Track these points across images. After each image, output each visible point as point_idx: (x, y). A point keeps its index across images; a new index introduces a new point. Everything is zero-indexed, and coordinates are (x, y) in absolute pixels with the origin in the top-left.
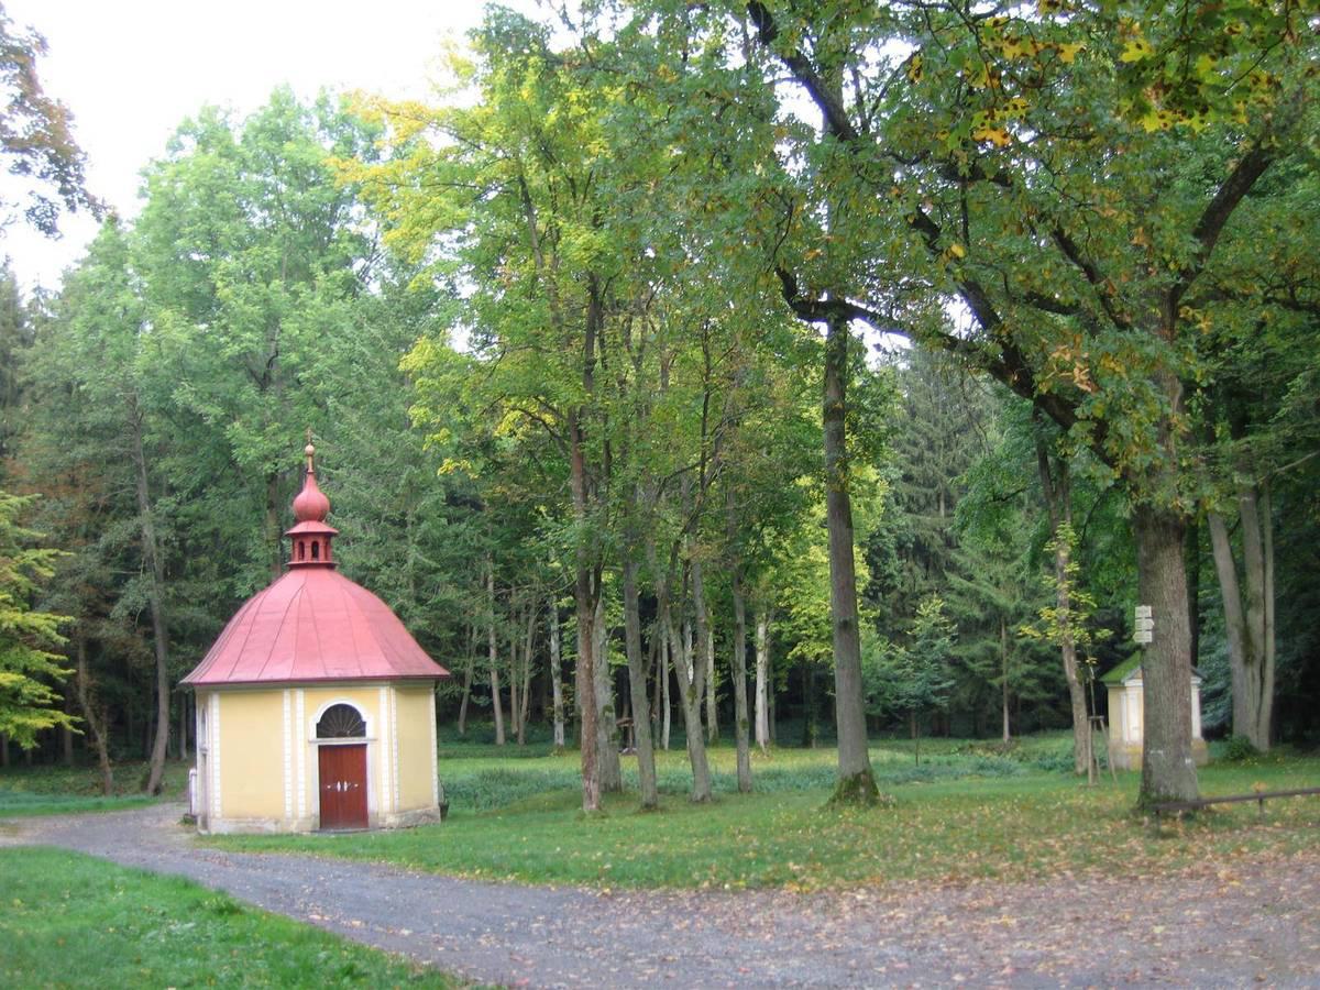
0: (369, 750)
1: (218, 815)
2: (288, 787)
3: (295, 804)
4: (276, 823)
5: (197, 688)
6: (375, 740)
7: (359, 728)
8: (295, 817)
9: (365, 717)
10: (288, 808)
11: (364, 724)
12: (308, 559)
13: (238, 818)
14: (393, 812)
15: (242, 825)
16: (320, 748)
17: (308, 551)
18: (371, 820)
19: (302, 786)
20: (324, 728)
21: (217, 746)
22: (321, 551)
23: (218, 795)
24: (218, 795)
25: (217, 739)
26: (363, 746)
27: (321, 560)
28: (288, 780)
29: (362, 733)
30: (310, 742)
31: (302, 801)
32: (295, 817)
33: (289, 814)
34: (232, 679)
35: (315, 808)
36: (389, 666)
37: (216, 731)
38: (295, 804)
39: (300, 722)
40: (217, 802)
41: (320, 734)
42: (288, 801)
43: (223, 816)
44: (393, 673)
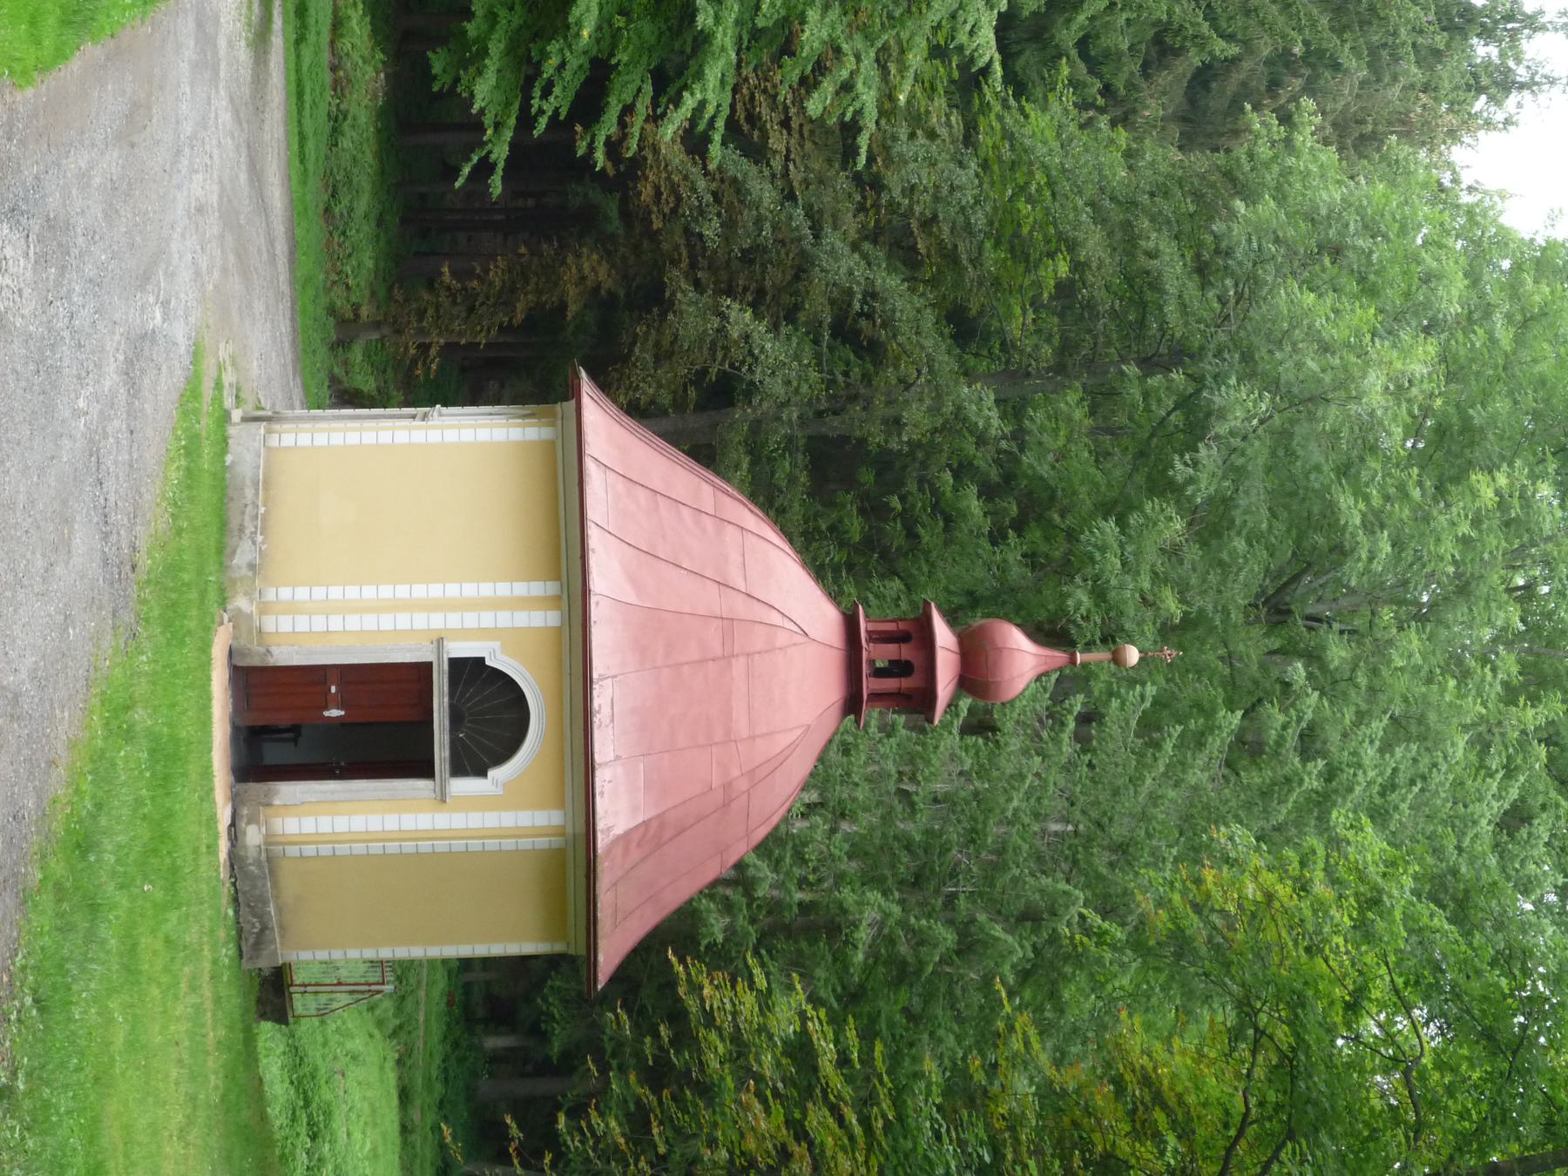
0: (421, 784)
1: (274, 441)
2: (335, 592)
3: (293, 608)
4: (252, 566)
5: (573, 402)
7: (471, 762)
8: (264, 609)
10: (285, 593)
11: (481, 772)
13: (266, 484)
14: (270, 840)
15: (249, 493)
16: (431, 664)
18: (255, 788)
19: (336, 623)
20: (469, 671)
21: (434, 436)
22: (890, 684)
23: (321, 439)
24: (321, 439)
25: (451, 436)
26: (424, 769)
27: (868, 685)
28: (352, 592)
29: (458, 770)
30: (440, 642)
31: (302, 624)
32: (264, 609)
33: (270, 595)
34: (590, 467)
35: (286, 655)
36: (619, 830)
37: (467, 435)
38: (293, 608)
39: (487, 619)
40: (304, 439)
41: (457, 665)
42: (302, 593)
43: (269, 450)
44: (602, 842)
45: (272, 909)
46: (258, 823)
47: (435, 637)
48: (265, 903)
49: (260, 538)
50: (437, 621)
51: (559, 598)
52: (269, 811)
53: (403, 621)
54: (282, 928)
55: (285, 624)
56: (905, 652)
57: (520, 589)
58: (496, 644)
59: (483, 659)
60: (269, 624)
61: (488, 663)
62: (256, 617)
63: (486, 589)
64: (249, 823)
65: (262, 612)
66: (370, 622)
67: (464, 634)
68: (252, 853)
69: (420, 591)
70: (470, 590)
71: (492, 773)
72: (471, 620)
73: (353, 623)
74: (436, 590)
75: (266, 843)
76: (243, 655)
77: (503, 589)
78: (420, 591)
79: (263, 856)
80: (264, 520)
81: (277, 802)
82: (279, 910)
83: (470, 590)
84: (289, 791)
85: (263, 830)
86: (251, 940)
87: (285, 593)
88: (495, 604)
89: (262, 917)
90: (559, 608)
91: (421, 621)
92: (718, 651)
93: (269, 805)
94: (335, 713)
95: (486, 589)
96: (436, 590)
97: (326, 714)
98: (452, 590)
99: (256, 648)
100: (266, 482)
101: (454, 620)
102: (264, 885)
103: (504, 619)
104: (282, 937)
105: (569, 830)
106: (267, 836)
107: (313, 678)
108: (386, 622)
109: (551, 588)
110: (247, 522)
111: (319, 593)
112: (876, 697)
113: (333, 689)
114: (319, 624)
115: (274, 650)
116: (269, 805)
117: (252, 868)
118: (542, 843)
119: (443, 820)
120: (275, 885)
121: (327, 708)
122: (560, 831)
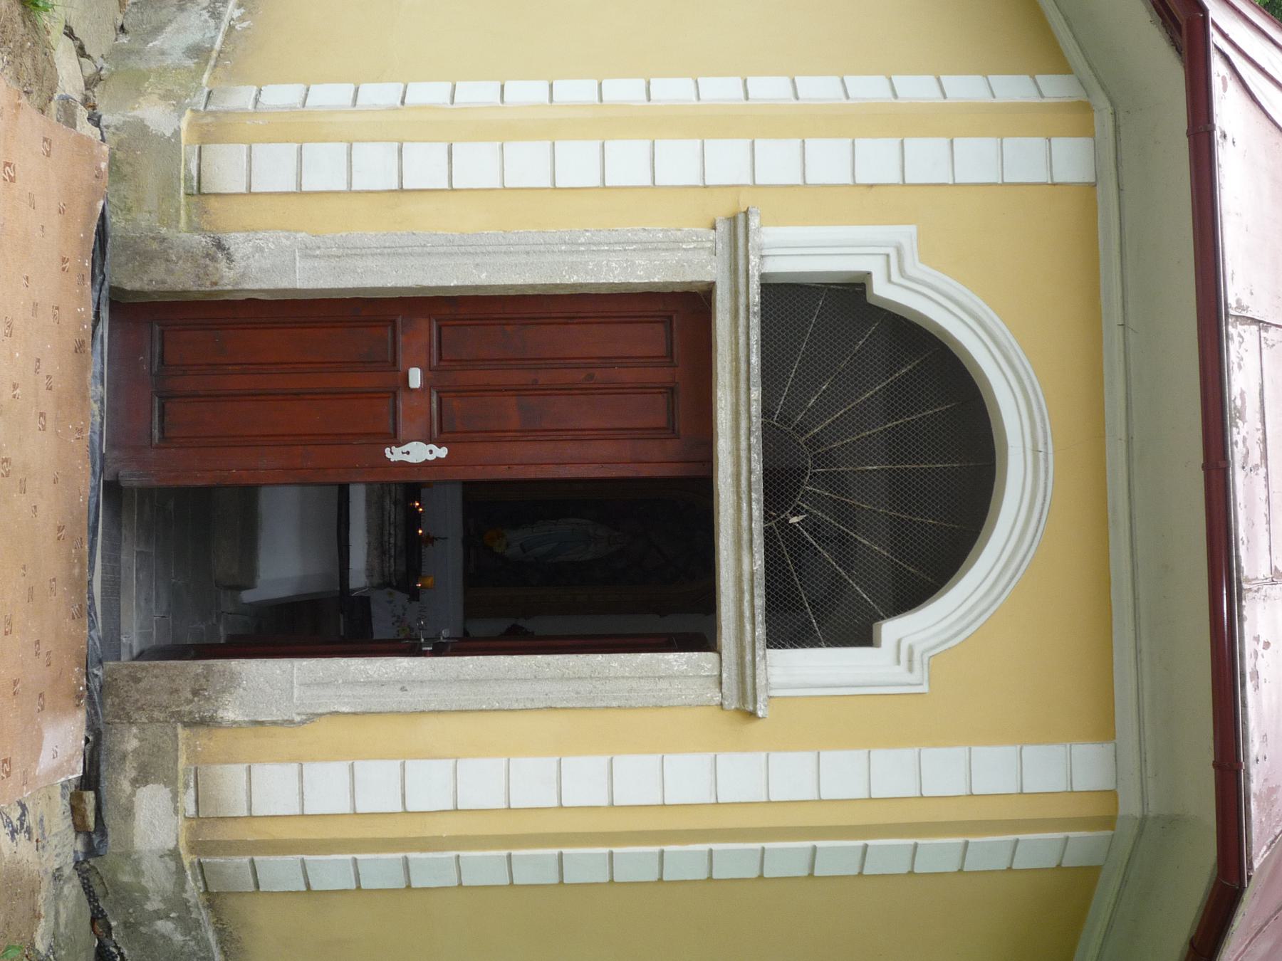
2: (428, 93)
4: (198, 52)
10: (280, 95)
42: (330, 95)
46: (170, 782)
47: (722, 208)
51: (1085, 108)
52: (205, 741)
58: (905, 234)
61: (883, 290)
64: (141, 779)
68: (156, 878)
71: (892, 629)
75: (197, 846)
76: (141, 254)
79: (193, 889)
81: (230, 713)
87: (280, 95)
90: (1087, 131)
93: (206, 722)
94: (418, 452)
97: (395, 454)
99: (184, 236)
106: (199, 820)
109: (1055, 87)
111: (379, 94)
113: (415, 378)
115: (238, 242)
116: (206, 722)
117: (164, 926)
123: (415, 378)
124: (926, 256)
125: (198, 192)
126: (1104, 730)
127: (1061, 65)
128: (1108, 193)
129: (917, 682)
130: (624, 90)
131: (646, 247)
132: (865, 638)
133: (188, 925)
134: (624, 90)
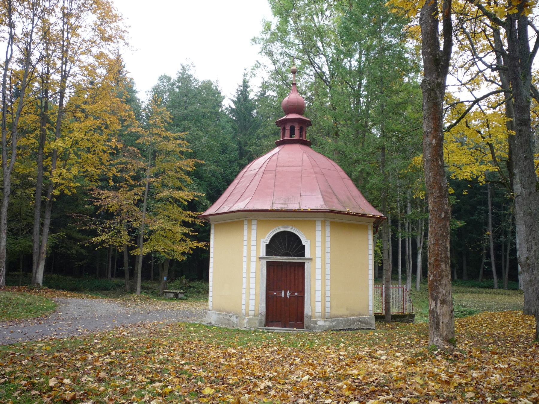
2: (244, 291)
3: (247, 305)
4: (237, 317)
6: (310, 260)
7: (300, 250)
9: (304, 241)
10: (243, 307)
12: (287, 137)
14: (323, 317)
15: (221, 316)
16: (267, 262)
17: (287, 133)
18: (306, 321)
19: (252, 292)
20: (271, 249)
22: (297, 132)
26: (302, 265)
29: (303, 255)
31: (252, 302)
33: (243, 312)
36: (322, 203)
38: (247, 305)
39: (254, 243)
41: (267, 254)
42: (244, 302)
45: (351, 318)
46: (317, 321)
48: (349, 320)
49: (231, 314)
50: (253, 259)
53: (253, 270)
54: (360, 315)
55: (252, 308)
56: (288, 127)
57: (245, 232)
58: (262, 240)
59: (267, 245)
60: (252, 313)
61: (267, 243)
62: (250, 317)
63: (245, 243)
64: (317, 324)
65: (249, 315)
66: (253, 281)
67: (258, 250)
68: (327, 324)
69: (245, 264)
70: (245, 248)
71: (303, 244)
72: (254, 248)
73: (253, 286)
74: (245, 259)
77: (245, 238)
78: (245, 264)
80: (227, 312)
81: (310, 314)
82: (352, 315)
83: (245, 248)
84: (307, 310)
85: (319, 319)
86: (364, 325)
87: (243, 307)
88: (249, 240)
89: (354, 321)
91: (253, 264)
92: (273, 175)
93: (311, 317)
95: (245, 243)
96: (245, 259)
98: (245, 254)
100: (220, 311)
101: (253, 254)
102: (341, 320)
103: (254, 238)
104: (363, 315)
105: (323, 219)
107: (270, 300)
108: (253, 275)
109: (246, 223)
110: (227, 318)
111: (244, 296)
112: (301, 135)
113: (275, 294)
114: (252, 297)
115: (260, 312)
116: (311, 317)
117: (334, 324)
118: (328, 229)
119: (318, 260)
120: (341, 316)
121: (281, 296)
122: (323, 223)
123: (275, 294)
124: (264, 238)
125: (254, 316)
126: (315, 221)
127: (243, 221)
128: (258, 218)
129: (309, 241)
130: (245, 270)
131: (262, 268)
132: (304, 246)
133: (334, 321)
134: (245, 270)
